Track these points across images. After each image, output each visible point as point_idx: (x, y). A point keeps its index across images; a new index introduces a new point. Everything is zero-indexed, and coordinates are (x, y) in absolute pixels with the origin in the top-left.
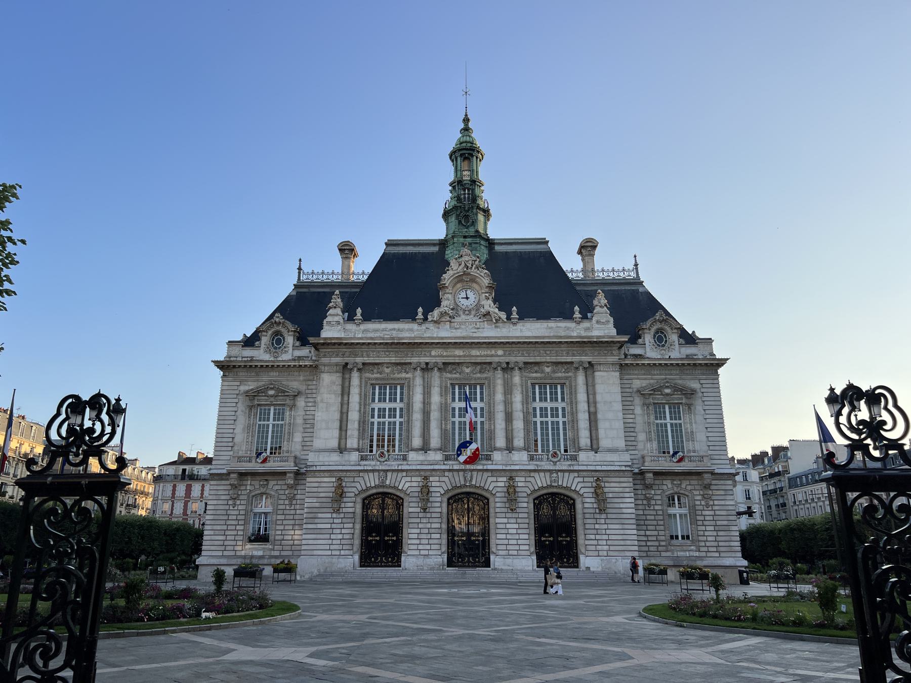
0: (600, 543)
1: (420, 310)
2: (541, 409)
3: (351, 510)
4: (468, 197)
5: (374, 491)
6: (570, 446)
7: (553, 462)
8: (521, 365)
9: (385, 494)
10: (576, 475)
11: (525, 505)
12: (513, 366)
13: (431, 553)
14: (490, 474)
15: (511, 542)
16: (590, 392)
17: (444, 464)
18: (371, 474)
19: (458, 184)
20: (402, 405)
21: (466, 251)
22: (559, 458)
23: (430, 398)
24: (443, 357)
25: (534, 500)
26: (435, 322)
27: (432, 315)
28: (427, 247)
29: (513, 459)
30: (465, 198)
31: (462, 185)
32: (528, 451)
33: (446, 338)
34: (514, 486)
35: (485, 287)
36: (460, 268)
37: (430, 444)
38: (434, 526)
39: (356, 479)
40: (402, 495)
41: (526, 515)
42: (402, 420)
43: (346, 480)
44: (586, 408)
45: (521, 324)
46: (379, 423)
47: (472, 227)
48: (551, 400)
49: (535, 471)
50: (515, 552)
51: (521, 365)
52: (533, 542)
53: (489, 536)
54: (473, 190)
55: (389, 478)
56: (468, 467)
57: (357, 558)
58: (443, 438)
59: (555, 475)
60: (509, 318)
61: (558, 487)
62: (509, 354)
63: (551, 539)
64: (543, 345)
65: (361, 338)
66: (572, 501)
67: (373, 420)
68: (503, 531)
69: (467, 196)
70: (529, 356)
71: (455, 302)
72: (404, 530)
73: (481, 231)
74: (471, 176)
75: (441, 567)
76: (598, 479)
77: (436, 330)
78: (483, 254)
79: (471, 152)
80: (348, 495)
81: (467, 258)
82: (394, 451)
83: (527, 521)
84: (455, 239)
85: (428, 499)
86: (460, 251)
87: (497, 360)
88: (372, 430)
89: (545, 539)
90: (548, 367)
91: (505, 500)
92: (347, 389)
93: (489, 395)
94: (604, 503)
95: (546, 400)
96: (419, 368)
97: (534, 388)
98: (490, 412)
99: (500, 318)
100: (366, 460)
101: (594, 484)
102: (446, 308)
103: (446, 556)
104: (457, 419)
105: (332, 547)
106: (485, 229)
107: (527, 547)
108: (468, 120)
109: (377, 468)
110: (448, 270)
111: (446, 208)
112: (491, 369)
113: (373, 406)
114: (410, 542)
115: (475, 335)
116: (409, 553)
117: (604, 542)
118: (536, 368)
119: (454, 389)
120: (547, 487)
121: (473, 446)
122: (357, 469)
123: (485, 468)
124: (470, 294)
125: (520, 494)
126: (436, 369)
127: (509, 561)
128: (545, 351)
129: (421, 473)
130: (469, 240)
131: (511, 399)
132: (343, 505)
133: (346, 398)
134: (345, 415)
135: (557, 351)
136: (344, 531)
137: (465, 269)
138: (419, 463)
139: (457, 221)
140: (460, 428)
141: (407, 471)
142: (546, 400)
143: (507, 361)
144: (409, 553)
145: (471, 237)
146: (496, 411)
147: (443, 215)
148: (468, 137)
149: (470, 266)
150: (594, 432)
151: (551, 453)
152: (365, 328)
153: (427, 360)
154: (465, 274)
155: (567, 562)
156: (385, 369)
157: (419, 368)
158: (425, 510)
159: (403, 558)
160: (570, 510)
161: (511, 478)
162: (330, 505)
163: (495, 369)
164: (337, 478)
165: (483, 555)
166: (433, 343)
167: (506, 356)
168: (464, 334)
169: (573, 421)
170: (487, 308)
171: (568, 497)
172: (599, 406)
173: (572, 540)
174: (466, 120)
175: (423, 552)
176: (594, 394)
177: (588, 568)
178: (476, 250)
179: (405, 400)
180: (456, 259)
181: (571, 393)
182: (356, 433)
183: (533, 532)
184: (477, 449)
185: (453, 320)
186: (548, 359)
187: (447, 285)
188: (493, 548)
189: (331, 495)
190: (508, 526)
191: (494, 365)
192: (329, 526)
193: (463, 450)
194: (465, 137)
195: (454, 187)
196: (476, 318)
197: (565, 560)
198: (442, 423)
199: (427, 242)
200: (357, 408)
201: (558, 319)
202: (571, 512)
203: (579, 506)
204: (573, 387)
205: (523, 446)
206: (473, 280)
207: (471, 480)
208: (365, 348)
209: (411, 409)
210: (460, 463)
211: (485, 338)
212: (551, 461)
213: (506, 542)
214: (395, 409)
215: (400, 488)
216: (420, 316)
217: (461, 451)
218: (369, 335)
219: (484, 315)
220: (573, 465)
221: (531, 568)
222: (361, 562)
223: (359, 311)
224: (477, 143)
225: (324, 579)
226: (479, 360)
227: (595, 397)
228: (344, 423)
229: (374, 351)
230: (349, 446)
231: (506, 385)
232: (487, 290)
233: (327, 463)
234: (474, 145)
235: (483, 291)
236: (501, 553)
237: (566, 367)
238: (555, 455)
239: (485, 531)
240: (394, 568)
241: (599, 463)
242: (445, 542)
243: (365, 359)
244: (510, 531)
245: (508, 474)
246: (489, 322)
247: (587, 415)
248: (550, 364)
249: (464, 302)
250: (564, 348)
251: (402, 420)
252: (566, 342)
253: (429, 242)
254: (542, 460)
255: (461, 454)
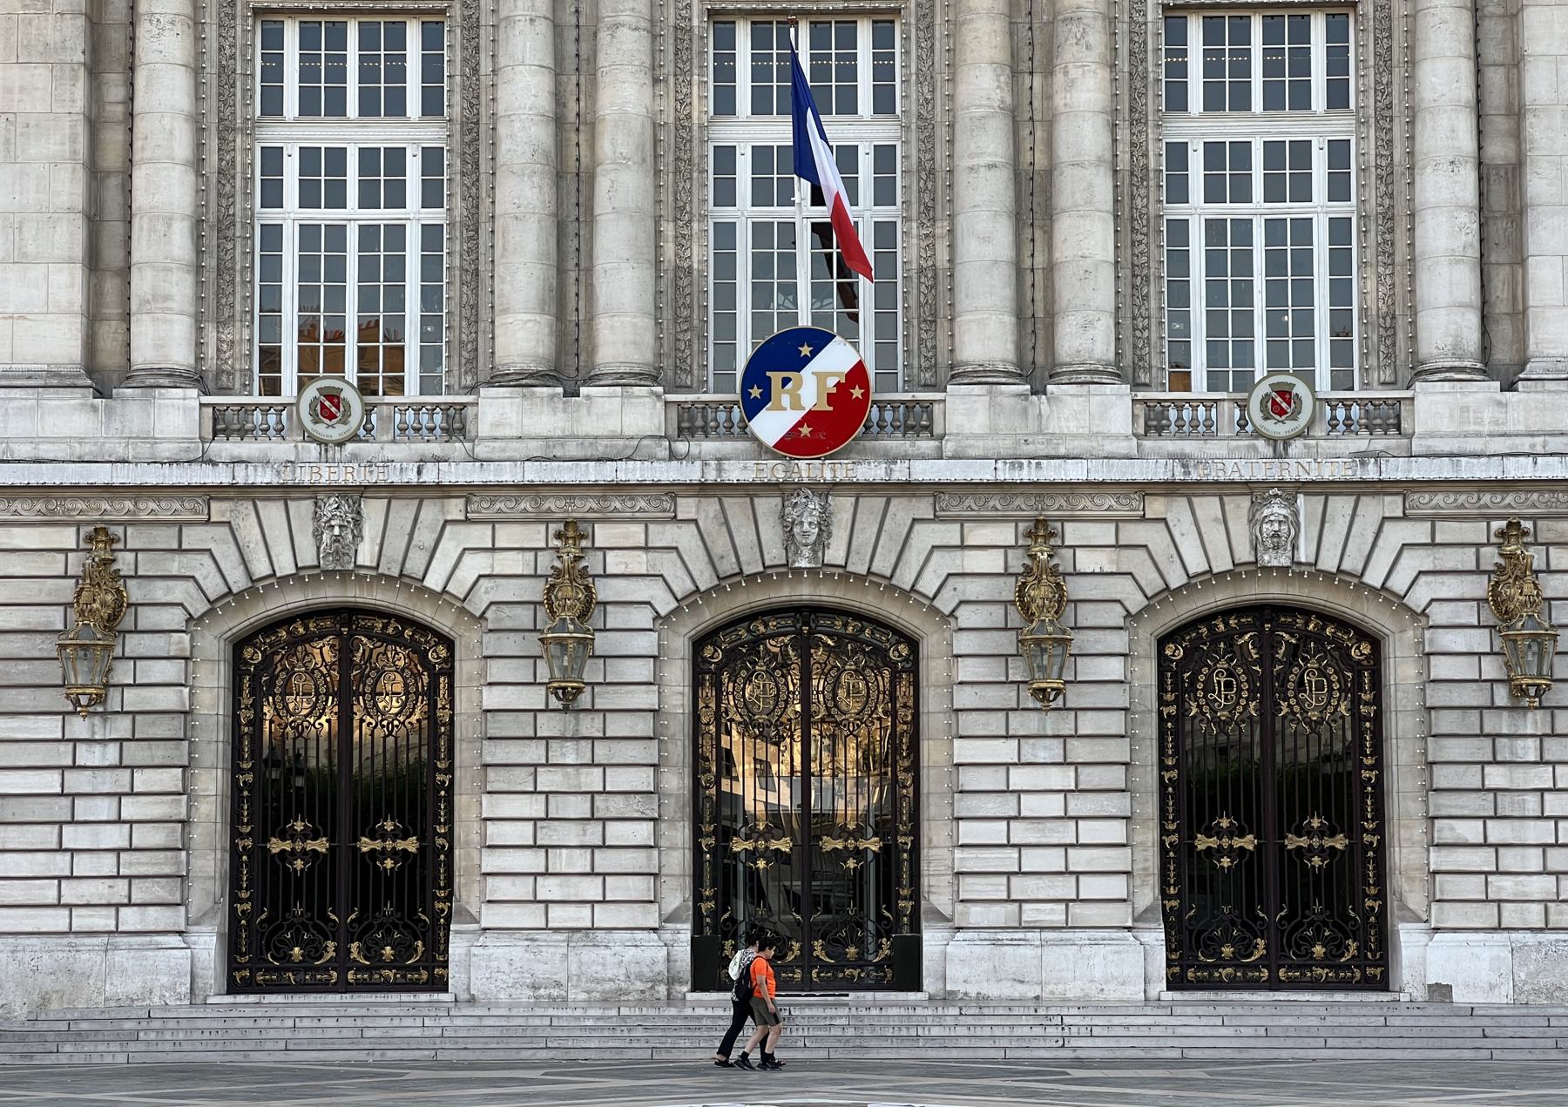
0: (1510, 860)
2: (1213, 151)
3: (168, 699)
5: (295, 599)
6: (1365, 356)
7: (1272, 440)
9: (346, 618)
10: (1393, 505)
11: (1114, 669)
13: (604, 916)
14: (924, 508)
15: (1033, 860)
16: (1492, 53)
17: (673, 456)
18: (272, 512)
20: (433, 134)
22: (1304, 418)
23: (593, 96)
25: (1162, 642)
29: (1053, 427)
32: (1137, 385)
34: (1054, 571)
37: (592, 352)
38: (620, 780)
39: (192, 537)
40: (444, 621)
41: (1115, 723)
42: (436, 216)
43: (135, 538)
44: (1467, 143)
46: (308, 234)
48: (1273, 101)
49: (1170, 488)
50: (1056, 914)
52: (1150, 860)
53: (915, 832)
55: (371, 529)
56: (806, 469)
57: (208, 945)
58: (668, 314)
59: (1277, 510)
61: (1292, 572)
63: (1248, 842)
66: (1366, 649)
67: (271, 216)
68: (991, 806)
72: (461, 801)
75: (662, 990)
76: (1513, 530)
80: (148, 618)
82: (397, 385)
83: (1120, 751)
85: (585, 643)
88: (272, 268)
89: (1213, 842)
91: (1006, 642)
92: (116, 37)
93: (926, 77)
94: (1541, 655)
95: (1241, 102)
97: (1176, 36)
98: (932, 172)
100: (243, 433)
101: (1491, 557)
103: (683, 935)
104: (744, 212)
105: (71, 892)
107: (1117, 887)
109: (305, 477)
113: (272, 134)
114: (491, 862)
116: (490, 917)
117: (1533, 860)
119: (725, 41)
120: (1235, 574)
121: (836, 359)
122: (196, 481)
123: (900, 473)
125: (1088, 615)
127: (1020, 956)
129: (550, 504)
131: (1048, 96)
132: (123, 673)
133: (114, 92)
134: (113, 184)
136: (131, 809)
138: (535, 448)
140: (761, 265)
141: (467, 491)
142: (1241, 102)
144: (490, 917)
146: (963, 163)
150: (1500, 277)
151: (1263, 389)
155: (1330, 961)
158: (567, 697)
159: (457, 948)
160: (1353, 691)
161: (1041, 530)
162: (53, 672)
164: (85, 530)
165: (885, 928)
169: (1388, 217)
171: (1343, 624)
172: (1538, 130)
173: (1356, 849)
175: (560, 917)
176: (1516, 63)
177: (1441, 992)
179: (454, 104)
181: (1384, 61)
182: (181, 288)
183: (1150, 807)
184: (857, 374)
188: (936, 891)
189: (55, 618)
190: (1019, 778)
192: (50, 782)
193: (776, 377)
197: (1319, 950)
198: (658, 233)
200: (182, 146)
202: (1356, 703)
203: (1401, 672)
204: (1399, 27)
205: (1111, 356)
207: (821, 543)
209: (484, 156)
210: (762, 451)
212: (1258, 434)
213: (1007, 861)
214: (396, 158)
215: (434, 581)
217: (766, 385)
220: (1377, 456)
221: (1135, 992)
222: (232, 965)
225: (24, 1055)
227: (1515, 84)
228: (114, 230)
230: (144, 353)
231: (1022, 19)
233: (23, 451)
236: (976, 914)
238: (1281, 402)
239: (896, 810)
240: (405, 997)
241: (1524, 444)
242: (678, 860)
244: (1031, 805)
245: (1025, 507)
247: (1467, 179)
251: (436, 216)
254: (1209, 431)
255: (766, 398)
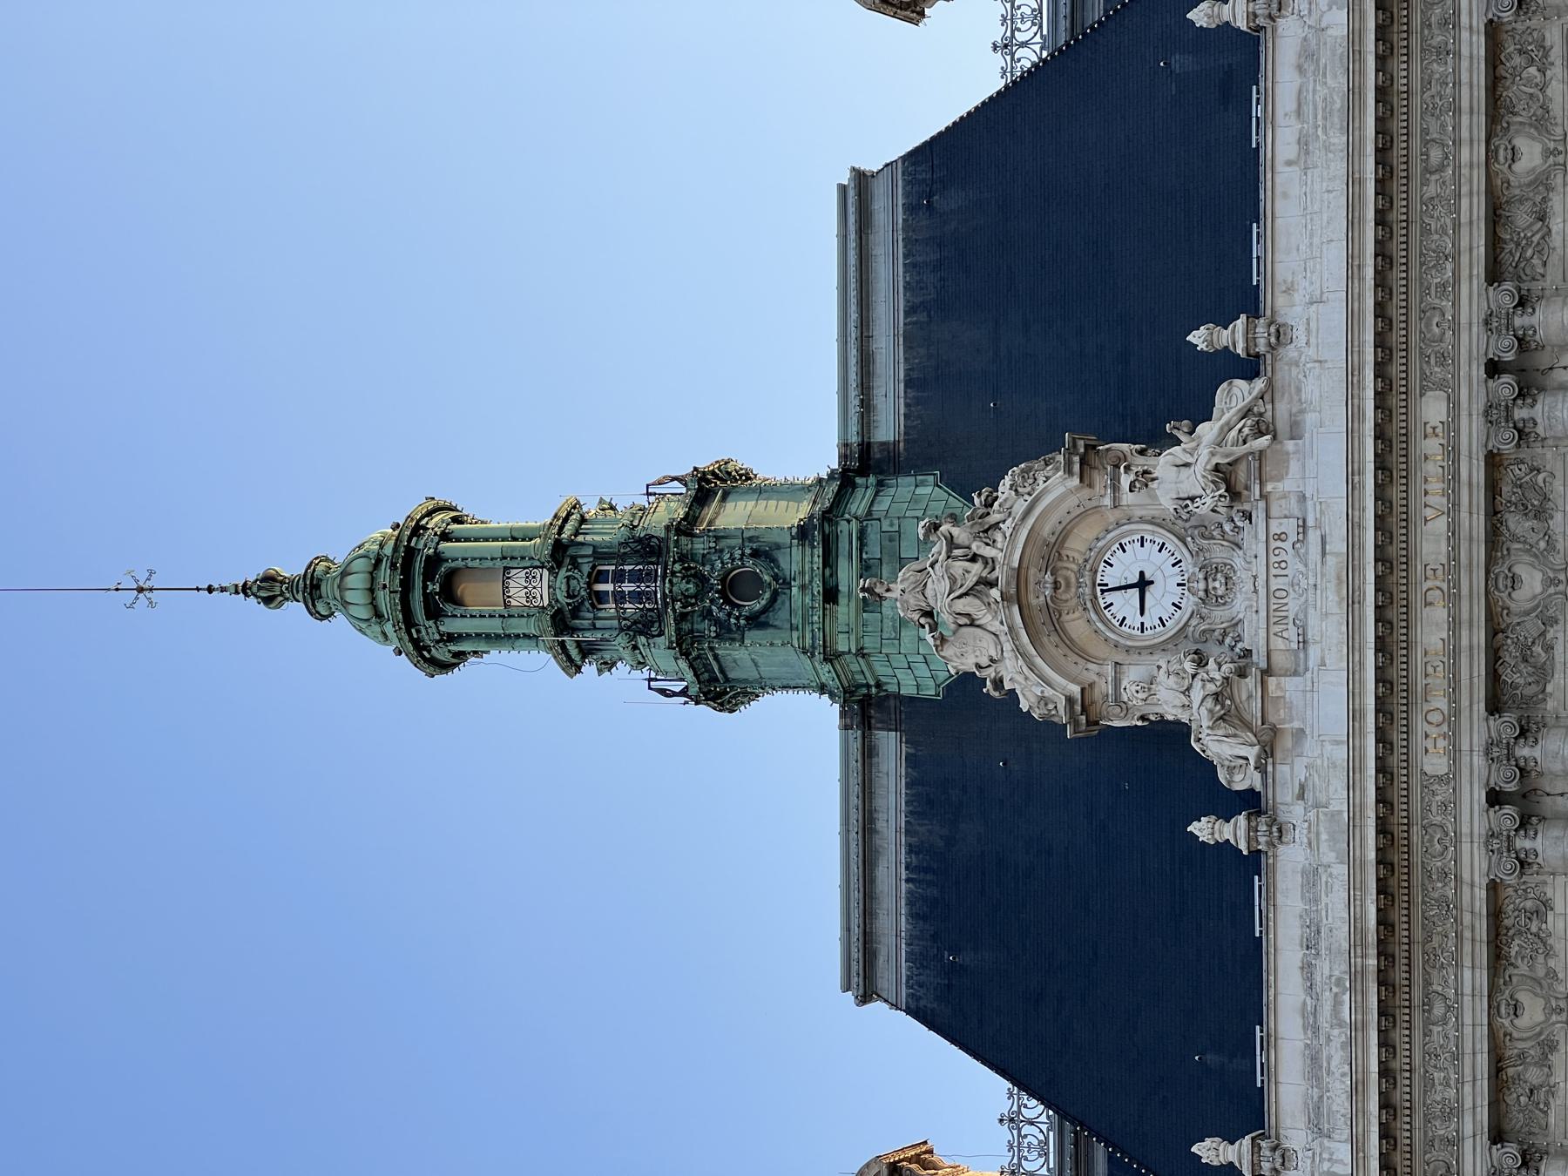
1: (1203, 829)
4: (636, 577)
8: (1504, 297)
12: (1508, 341)
19: (572, 631)
21: (900, 591)
24: (1456, 712)
26: (1268, 751)
27: (1231, 770)
28: (880, 791)
30: (637, 597)
31: (576, 612)
33: (1353, 694)
35: (1086, 492)
36: (985, 618)
45: (1281, 300)
47: (784, 563)
51: (1504, 297)
54: (599, 554)
60: (1250, 367)
62: (1442, 358)
64: (1396, 187)
65: (1358, 1146)
69: (628, 587)
70: (1456, 257)
71: (1162, 647)
73: (798, 512)
74: (530, 564)
77: (1310, 747)
78: (914, 499)
79: (419, 566)
81: (938, 587)
84: (842, 647)
86: (903, 623)
87: (1478, 423)
90: (1514, 155)
96: (1522, 843)
99: (1246, 413)
102: (1197, 694)
106: (789, 491)
108: (269, 579)
110: (998, 683)
111: (683, 693)
112: (1524, 453)
115: (1338, 545)
118: (1522, 217)
124: (1122, 569)
126: (1523, 751)
128: (1428, 170)
130: (846, 573)
135: (1430, 111)
137: (995, 593)
139: (752, 636)
143: (1479, 372)
145: (829, 560)
147: (721, 708)
148: (351, 581)
149: (977, 569)
152: (1301, 1122)
153: (1473, 797)
154: (1017, 597)
156: (1524, 1021)
157: (1522, 843)
163: (1523, 434)
166: (1382, 768)
167: (1456, 376)
168: (1332, 600)
170: (1195, 481)
174: (269, 590)
178: (895, 537)
180: (943, 639)
185: (1259, 659)
186: (1472, 153)
187: (1075, 690)
191: (1505, 441)
194: (349, 596)
195: (586, 651)
196: (1246, 535)
199: (856, 789)
201: (1257, 111)
206: (1050, 552)
208: (1414, 1130)
211: (1353, 487)
216: (1234, 831)
218: (1339, 1101)
219: (1234, 494)
223: (1209, 1150)
224: (377, 535)
226: (1474, 523)
229: (1429, 1083)
232: (1101, 480)
234: (388, 550)
235: (1107, 501)
237: (1518, 60)
243: (1468, 1129)
246: (1268, 469)
248: (1500, 143)
249: (1161, 599)
250: (1411, 72)
252: (1382, 61)
253: (855, 780)
